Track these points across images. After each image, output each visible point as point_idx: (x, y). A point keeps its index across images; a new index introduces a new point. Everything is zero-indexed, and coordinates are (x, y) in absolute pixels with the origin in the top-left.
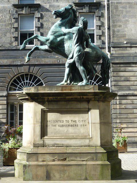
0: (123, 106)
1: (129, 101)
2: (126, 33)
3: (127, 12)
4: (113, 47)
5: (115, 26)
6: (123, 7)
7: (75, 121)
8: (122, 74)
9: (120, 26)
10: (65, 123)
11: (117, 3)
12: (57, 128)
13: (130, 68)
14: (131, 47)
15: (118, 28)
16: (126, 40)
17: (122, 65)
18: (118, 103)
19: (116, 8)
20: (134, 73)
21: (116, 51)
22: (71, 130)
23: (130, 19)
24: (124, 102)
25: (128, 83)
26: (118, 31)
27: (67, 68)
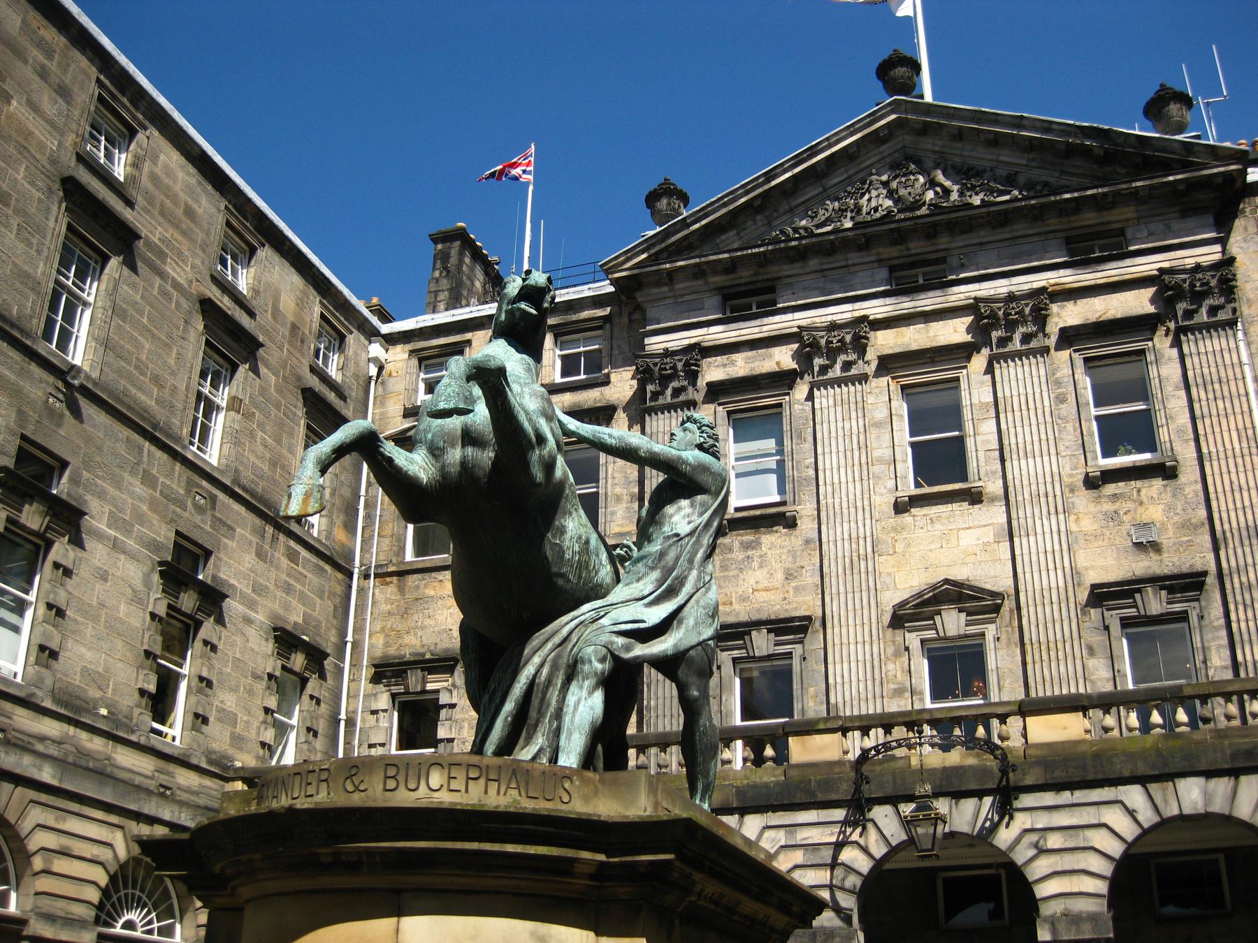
27: (595, 688)
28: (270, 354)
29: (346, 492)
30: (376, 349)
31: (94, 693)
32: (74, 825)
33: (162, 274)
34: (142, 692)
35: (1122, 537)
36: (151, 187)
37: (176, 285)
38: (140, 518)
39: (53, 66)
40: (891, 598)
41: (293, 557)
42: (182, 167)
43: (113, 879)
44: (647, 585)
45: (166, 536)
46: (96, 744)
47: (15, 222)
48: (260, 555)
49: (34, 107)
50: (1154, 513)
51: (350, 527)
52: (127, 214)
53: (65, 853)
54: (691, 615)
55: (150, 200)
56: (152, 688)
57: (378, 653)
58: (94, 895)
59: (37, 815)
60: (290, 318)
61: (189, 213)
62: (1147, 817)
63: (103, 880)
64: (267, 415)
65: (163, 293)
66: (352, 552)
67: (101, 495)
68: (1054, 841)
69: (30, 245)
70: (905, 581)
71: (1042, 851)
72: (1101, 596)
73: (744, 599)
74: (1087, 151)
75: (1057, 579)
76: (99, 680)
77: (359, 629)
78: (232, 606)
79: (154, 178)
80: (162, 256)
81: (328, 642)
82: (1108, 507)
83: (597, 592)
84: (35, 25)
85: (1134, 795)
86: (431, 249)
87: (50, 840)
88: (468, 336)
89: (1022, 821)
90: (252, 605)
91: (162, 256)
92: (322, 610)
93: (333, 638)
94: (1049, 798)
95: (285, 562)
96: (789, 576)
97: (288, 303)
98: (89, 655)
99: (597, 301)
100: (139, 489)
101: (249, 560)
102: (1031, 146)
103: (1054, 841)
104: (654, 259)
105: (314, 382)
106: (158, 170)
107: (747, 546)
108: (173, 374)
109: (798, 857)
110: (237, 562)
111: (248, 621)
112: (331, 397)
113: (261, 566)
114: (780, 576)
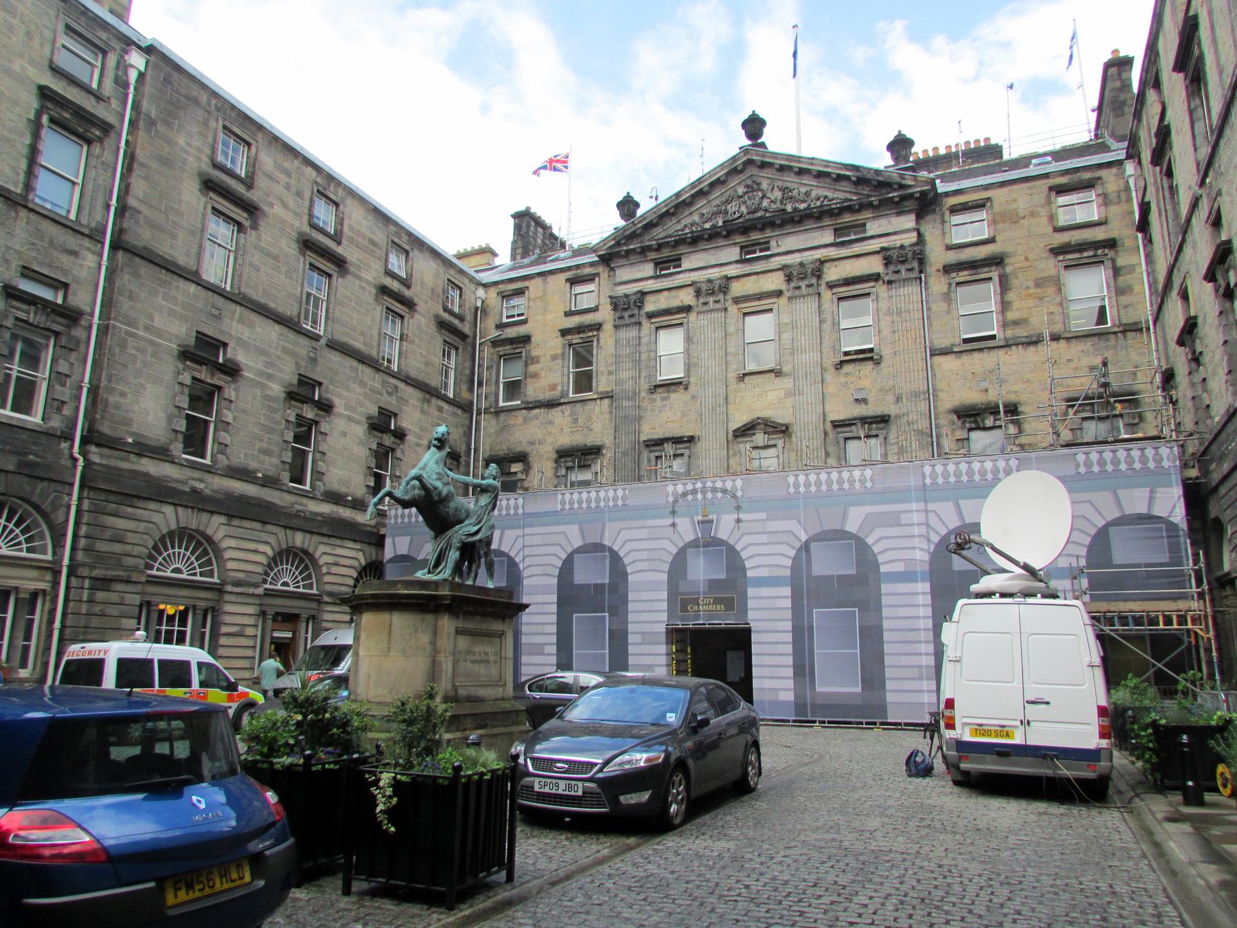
0: (97, 609)
1: (114, 597)
2: (132, 416)
3: (145, 364)
4: (98, 445)
5: (111, 391)
6: (137, 349)
7: (487, 654)
8: (109, 520)
9: (123, 395)
10: (476, 657)
11: (127, 333)
12: (469, 665)
13: (130, 510)
14: (140, 455)
15: (118, 399)
16: (132, 434)
17: (112, 498)
18: (85, 598)
19: (123, 345)
20: (137, 523)
21: (102, 456)
22: (482, 669)
23: (148, 385)
24: (100, 595)
25: (118, 548)
26: (117, 407)
28: (421, 307)
29: (467, 372)
30: (481, 292)
31: (343, 490)
32: (339, 551)
34: (368, 486)
36: (350, 234)
37: (368, 282)
38: (360, 404)
39: (292, 182)
40: (735, 425)
41: (440, 409)
42: (365, 218)
43: (360, 574)
44: (473, 521)
45: (374, 411)
47: (283, 269)
48: (422, 412)
49: (285, 205)
50: (866, 383)
51: (471, 390)
52: (340, 250)
53: (336, 564)
54: (483, 530)
55: (351, 240)
56: (372, 484)
57: (487, 454)
58: (351, 582)
59: (322, 548)
60: (430, 285)
65: (362, 288)
66: (472, 403)
67: (340, 396)
69: (291, 279)
70: (740, 419)
72: (836, 425)
73: (661, 426)
74: (847, 178)
75: (814, 418)
78: (410, 438)
80: (359, 268)
81: (462, 449)
82: (843, 379)
83: (461, 522)
84: (280, 161)
87: (329, 559)
88: (526, 284)
90: (420, 437)
91: (359, 268)
93: (464, 447)
95: (436, 413)
96: (683, 415)
97: (429, 279)
98: (340, 473)
99: (592, 264)
100: (357, 388)
101: (417, 415)
102: (820, 175)
104: (618, 244)
105: (446, 316)
106: (353, 223)
107: (664, 399)
108: (371, 328)
110: (413, 415)
111: (418, 445)
112: (456, 322)
113: (424, 417)
114: (679, 414)
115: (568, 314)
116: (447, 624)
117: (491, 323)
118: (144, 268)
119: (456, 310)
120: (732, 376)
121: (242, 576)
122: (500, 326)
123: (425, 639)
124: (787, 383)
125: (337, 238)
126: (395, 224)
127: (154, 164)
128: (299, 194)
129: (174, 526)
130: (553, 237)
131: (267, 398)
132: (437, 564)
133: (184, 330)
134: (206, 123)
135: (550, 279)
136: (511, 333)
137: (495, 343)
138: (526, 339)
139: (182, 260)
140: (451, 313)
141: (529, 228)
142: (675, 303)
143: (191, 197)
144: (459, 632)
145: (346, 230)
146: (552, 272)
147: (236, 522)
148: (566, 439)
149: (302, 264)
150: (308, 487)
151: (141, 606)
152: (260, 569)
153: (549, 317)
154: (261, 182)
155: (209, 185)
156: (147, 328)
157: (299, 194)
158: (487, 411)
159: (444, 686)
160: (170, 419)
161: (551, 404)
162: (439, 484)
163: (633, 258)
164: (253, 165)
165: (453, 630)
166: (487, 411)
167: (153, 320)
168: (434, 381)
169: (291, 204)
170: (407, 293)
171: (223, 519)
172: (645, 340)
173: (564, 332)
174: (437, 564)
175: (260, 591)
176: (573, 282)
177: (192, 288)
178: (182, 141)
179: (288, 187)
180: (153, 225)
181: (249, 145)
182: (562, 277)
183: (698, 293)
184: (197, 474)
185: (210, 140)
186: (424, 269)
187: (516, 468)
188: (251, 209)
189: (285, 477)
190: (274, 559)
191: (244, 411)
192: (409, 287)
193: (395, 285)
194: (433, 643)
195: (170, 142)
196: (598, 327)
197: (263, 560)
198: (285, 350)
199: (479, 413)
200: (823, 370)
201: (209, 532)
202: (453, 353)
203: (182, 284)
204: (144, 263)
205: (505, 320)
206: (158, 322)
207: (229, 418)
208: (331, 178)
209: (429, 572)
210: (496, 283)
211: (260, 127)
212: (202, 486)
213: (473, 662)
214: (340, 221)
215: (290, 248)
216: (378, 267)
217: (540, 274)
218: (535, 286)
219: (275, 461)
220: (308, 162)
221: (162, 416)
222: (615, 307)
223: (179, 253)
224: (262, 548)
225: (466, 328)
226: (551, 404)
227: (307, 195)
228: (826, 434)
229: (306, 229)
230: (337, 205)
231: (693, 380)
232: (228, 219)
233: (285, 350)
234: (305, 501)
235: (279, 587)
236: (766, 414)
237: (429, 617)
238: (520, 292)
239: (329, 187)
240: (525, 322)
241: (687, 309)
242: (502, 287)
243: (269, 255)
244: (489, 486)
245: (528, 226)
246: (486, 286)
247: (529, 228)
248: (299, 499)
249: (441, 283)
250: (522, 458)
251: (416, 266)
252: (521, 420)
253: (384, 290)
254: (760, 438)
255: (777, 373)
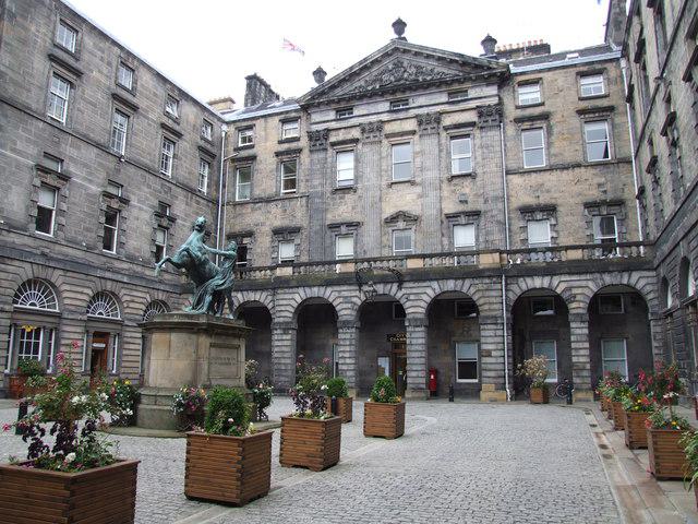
14: (9, 231)
28: (187, 137)
29: (215, 178)
30: (224, 127)
31: (137, 254)
32: (135, 293)
33: (147, 118)
35: (455, 198)
38: (147, 199)
39: (105, 56)
40: (385, 216)
41: (198, 203)
45: (156, 203)
46: (139, 269)
50: (467, 190)
52: (135, 101)
53: (133, 301)
55: (141, 93)
59: (123, 291)
60: (193, 123)
61: (155, 95)
62: (438, 291)
63: (144, 308)
64: (186, 157)
65: (150, 125)
67: (134, 194)
68: (412, 297)
70: (389, 211)
71: (408, 300)
72: (448, 217)
73: (339, 216)
74: (457, 61)
76: (139, 250)
77: (222, 223)
79: (142, 85)
80: (147, 111)
82: (453, 188)
83: (213, 277)
85: (435, 284)
86: (245, 82)
87: (128, 298)
89: (404, 291)
90: (185, 220)
91: (147, 111)
92: (210, 220)
94: (411, 285)
97: (191, 118)
99: (296, 111)
100: (146, 190)
101: (183, 206)
102: (440, 59)
103: (412, 297)
104: (313, 98)
105: (202, 143)
107: (341, 198)
109: (341, 300)
110: (180, 207)
112: (209, 147)
115: (280, 142)
116: (205, 341)
117: (231, 148)
118: (10, 111)
119: (210, 139)
120: (384, 183)
121: (73, 308)
122: (237, 149)
123: (192, 349)
124: (418, 190)
125: (132, 92)
126: (171, 83)
127: (15, 43)
128: (109, 64)
129: (31, 276)
130: (271, 91)
131: (88, 194)
132: (198, 304)
133: (36, 152)
134: (49, 17)
135: (270, 120)
136: (244, 153)
137: (233, 160)
138: (253, 158)
139: (34, 106)
140: (206, 140)
141: (257, 88)
142: (349, 137)
143: (40, 65)
144: (212, 345)
145: (139, 88)
146: (270, 115)
147: (69, 274)
148: (278, 223)
149: (110, 106)
150: (114, 253)
151: (10, 326)
152: (84, 304)
153: (268, 144)
154: (85, 56)
155: (52, 58)
156: (13, 150)
157: (109, 64)
158: (228, 204)
159: (203, 378)
160: (27, 208)
161: (268, 200)
162: (199, 254)
163: (323, 108)
164: (79, 44)
165: (208, 345)
166: (228, 204)
167: (15, 144)
168: (194, 185)
169: (105, 72)
170: (177, 128)
171: (61, 272)
172: (329, 160)
173: (278, 154)
174: (198, 304)
175: (85, 318)
176: (284, 122)
177: (41, 124)
178: (33, 29)
179: (102, 59)
180: (16, 84)
181: (77, 32)
182: (277, 119)
183: (363, 131)
184: (44, 244)
185: (52, 27)
186: (189, 111)
187: (246, 241)
188: (78, 74)
189: (100, 245)
190: (93, 298)
191: (74, 204)
192: (179, 124)
193: (170, 123)
194: (196, 352)
195: (27, 30)
196: (300, 151)
197: (87, 298)
198: (100, 164)
199: (223, 205)
200: (442, 181)
201: (53, 280)
202: (207, 166)
203: (34, 121)
204: (9, 108)
205: (240, 145)
206: (19, 146)
207: (65, 208)
208: (129, 54)
209: (193, 308)
210: (234, 122)
211: (84, 21)
212: (48, 251)
213: (222, 364)
214: (135, 82)
215: (101, 98)
216: (159, 110)
217: (262, 117)
218: (259, 124)
219: (94, 235)
220: (115, 43)
221: (23, 206)
222: (310, 138)
223: (32, 100)
224: (86, 291)
225: (214, 151)
226: (268, 200)
227: (114, 64)
228: (442, 222)
229: (113, 86)
230: (133, 71)
231: (359, 186)
232: (64, 80)
233: (100, 164)
234: (113, 261)
235: (97, 315)
236: (405, 209)
237: (194, 337)
238: (250, 128)
239: (129, 61)
240: (252, 147)
241: (356, 141)
242: (239, 124)
243: (91, 103)
244: (230, 255)
245: (256, 85)
246: (228, 123)
247: (257, 88)
248: (109, 260)
249: (200, 121)
250: (250, 234)
251: (183, 111)
252: (249, 210)
253: (163, 126)
254: (401, 224)
255: (412, 183)
